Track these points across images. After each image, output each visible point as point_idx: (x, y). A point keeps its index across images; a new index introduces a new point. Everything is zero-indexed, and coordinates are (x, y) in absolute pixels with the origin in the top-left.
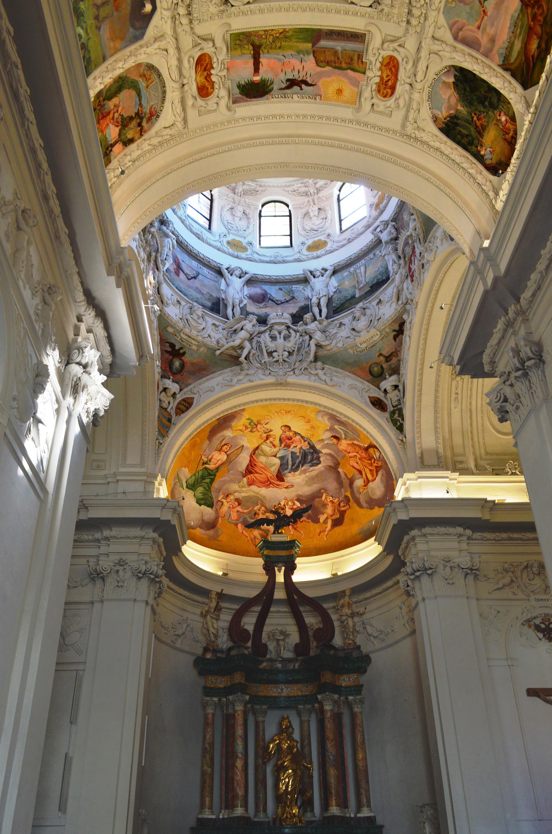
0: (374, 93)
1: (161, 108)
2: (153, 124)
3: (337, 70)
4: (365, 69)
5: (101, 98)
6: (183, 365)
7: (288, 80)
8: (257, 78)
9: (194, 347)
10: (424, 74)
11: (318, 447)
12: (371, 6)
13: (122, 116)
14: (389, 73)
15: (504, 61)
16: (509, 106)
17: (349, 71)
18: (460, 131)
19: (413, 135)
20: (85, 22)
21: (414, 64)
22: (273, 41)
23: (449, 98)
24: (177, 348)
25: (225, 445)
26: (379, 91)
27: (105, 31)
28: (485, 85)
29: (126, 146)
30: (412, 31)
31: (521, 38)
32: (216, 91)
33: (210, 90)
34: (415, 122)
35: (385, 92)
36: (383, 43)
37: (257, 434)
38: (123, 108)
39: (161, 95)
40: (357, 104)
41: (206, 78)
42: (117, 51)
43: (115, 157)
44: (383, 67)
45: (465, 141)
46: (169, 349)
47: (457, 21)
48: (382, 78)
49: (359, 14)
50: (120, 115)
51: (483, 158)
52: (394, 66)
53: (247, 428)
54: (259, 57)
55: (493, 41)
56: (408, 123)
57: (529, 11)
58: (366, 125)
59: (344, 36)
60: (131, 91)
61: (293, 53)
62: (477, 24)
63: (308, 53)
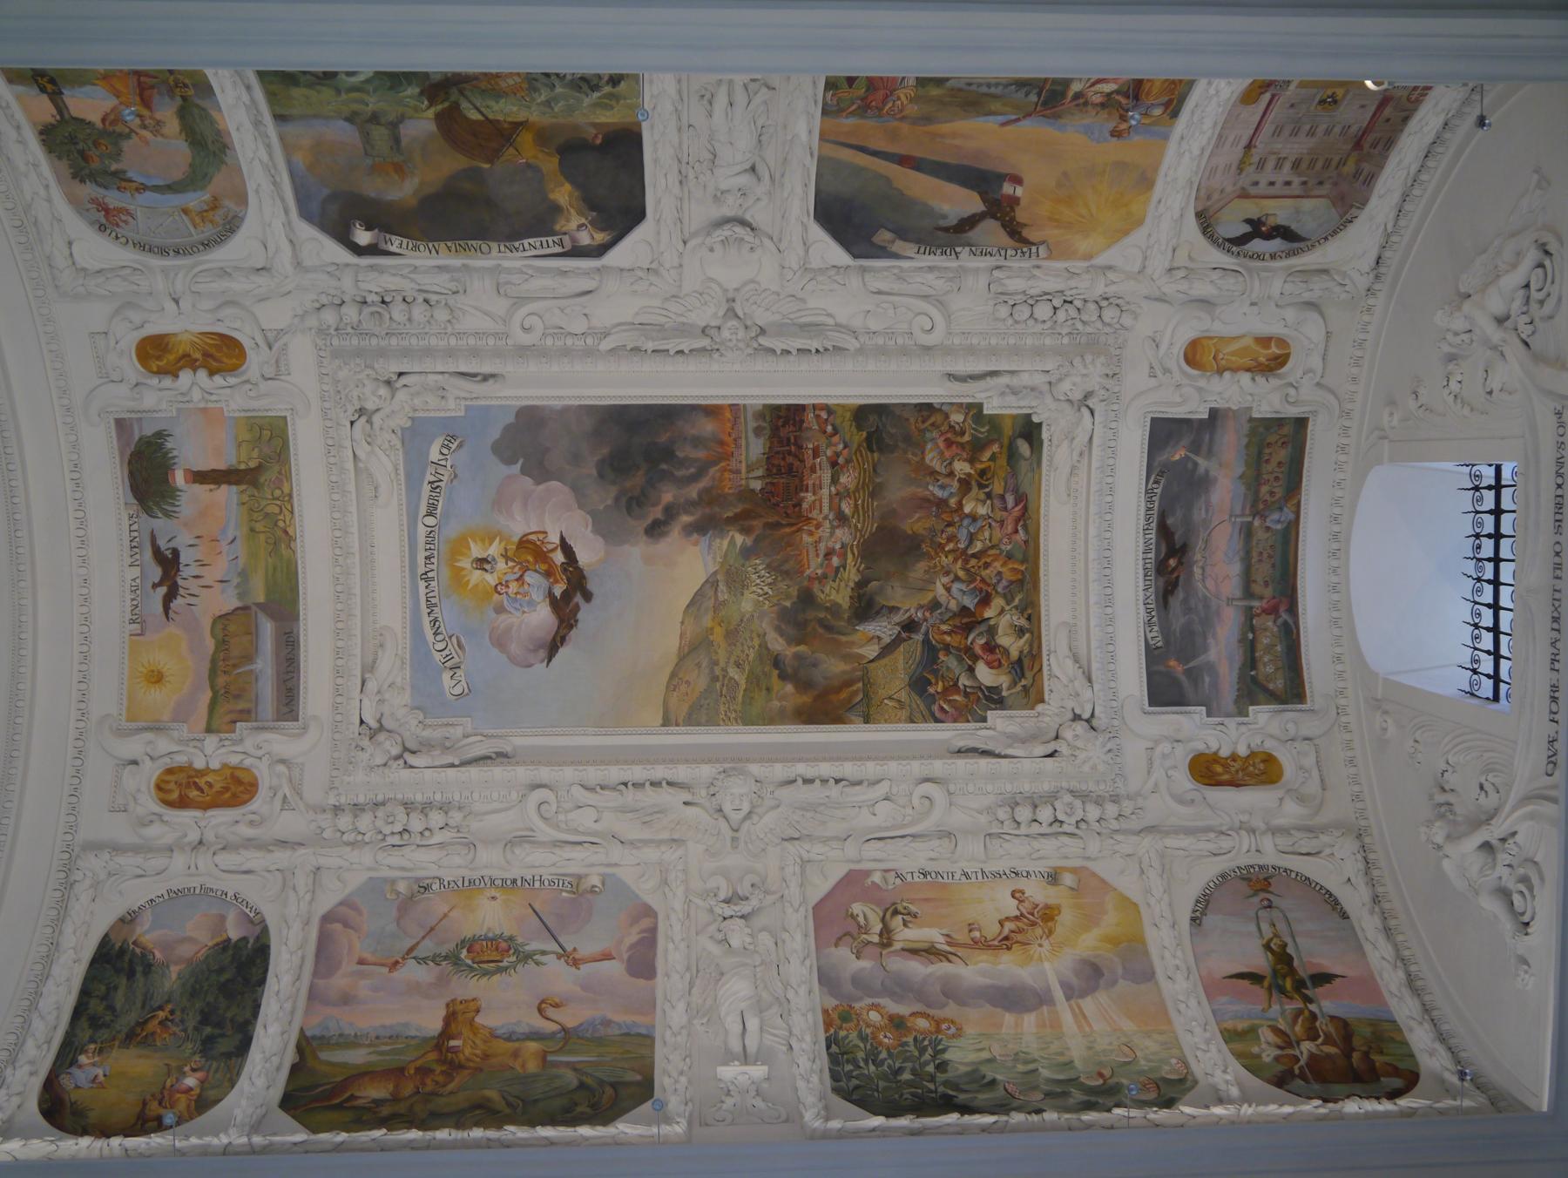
0: (167, 760)
1: (123, 240)
3: (206, 665)
4: (218, 731)
5: (191, 92)
7: (176, 552)
8: (179, 478)
10: (233, 868)
12: (362, 722)
13: (128, 137)
14: (218, 787)
15: (314, 1038)
16: (227, 1084)
17: (209, 694)
18: (116, 988)
19: (78, 876)
20: (375, 91)
21: (249, 840)
22: (267, 515)
23: (191, 940)
26: (170, 771)
27: (341, 133)
28: (248, 1015)
29: (41, 133)
30: (325, 820)
31: (374, 1058)
32: (154, 381)
33: (154, 365)
34: (110, 875)
35: (172, 786)
36: (283, 761)
38: (147, 143)
39: (158, 241)
40: (133, 725)
41: (186, 355)
42: (288, 148)
43: (18, 97)
44: (228, 772)
45: (96, 1006)
47: (360, 913)
48: (206, 771)
49: (339, 700)
50: (132, 131)
51: (71, 1065)
52: (234, 796)
54: (230, 483)
55: (346, 999)
56: (107, 856)
57: (433, 1056)
58: (80, 754)
59: (288, 672)
61: (241, 562)
62: (367, 956)
63: (241, 596)
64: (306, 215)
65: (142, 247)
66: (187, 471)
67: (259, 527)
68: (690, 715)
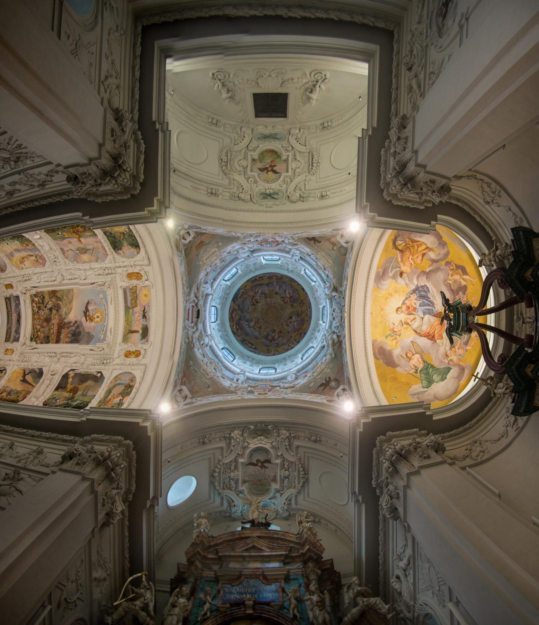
8: (141, 331)
11: (413, 287)
37: (403, 332)
53: (396, 338)
63: (133, 311)
68: (69, 292)
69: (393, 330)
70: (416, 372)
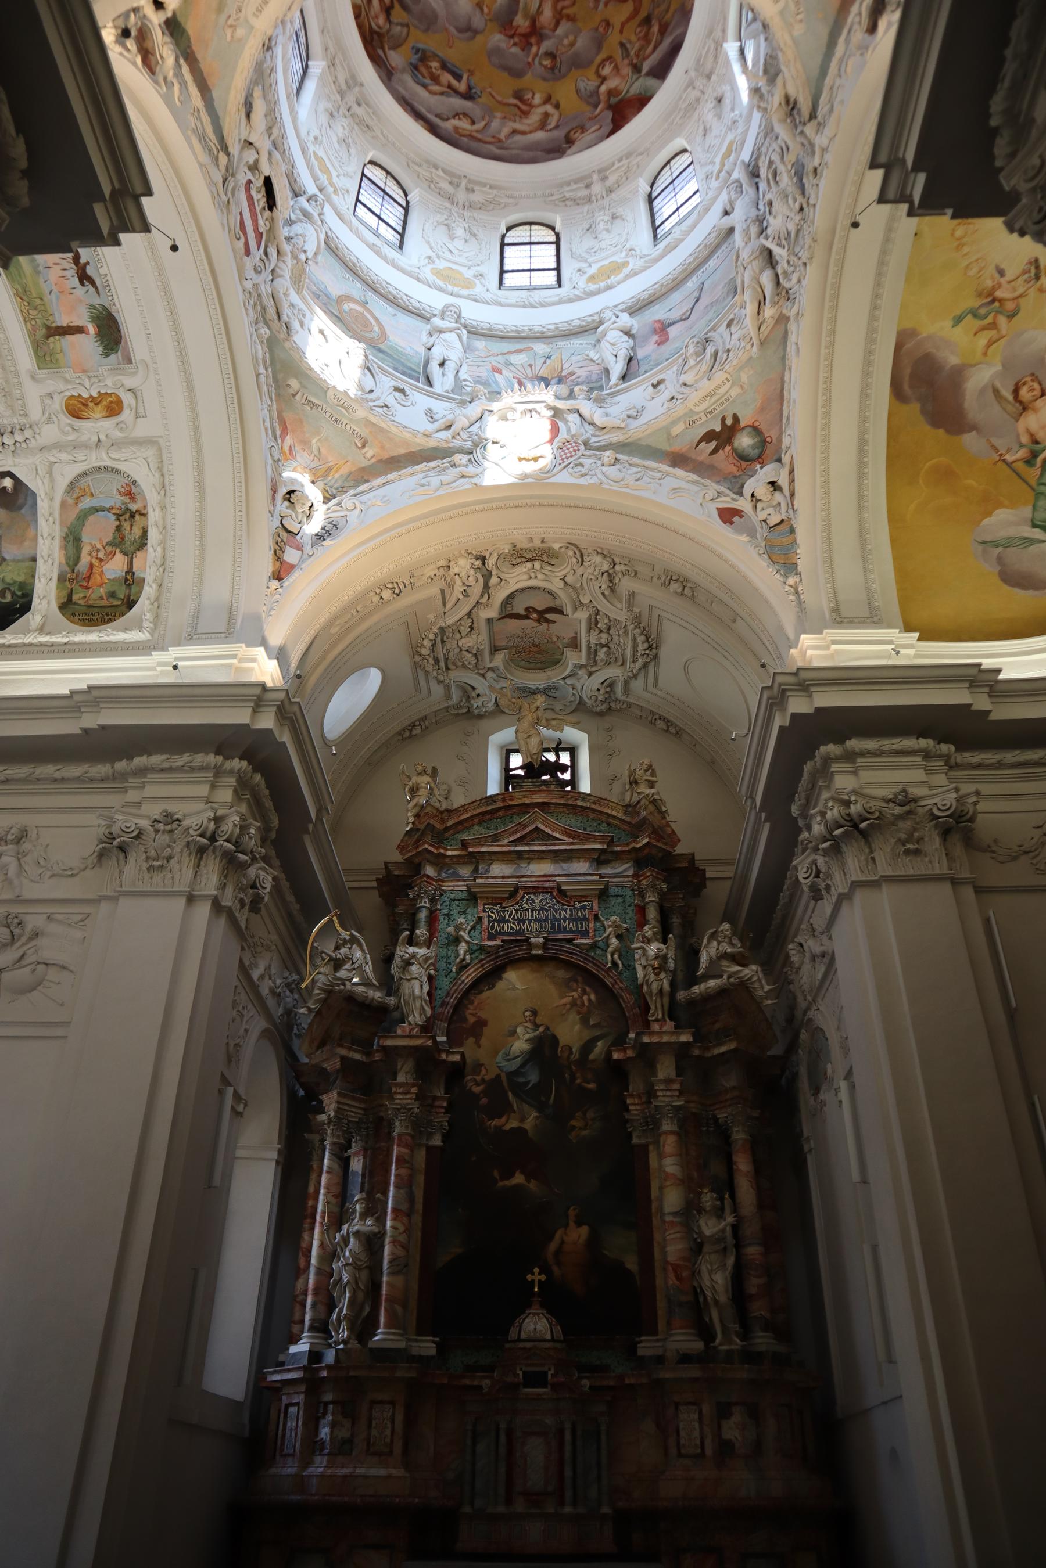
2: (141, 493)
6: (756, 430)
7: (83, 284)
8: (91, 328)
9: (734, 392)
13: (107, 544)
22: (36, 309)
24: (718, 429)
25: (1016, 391)
33: (113, 399)
39: (108, 475)
41: (96, 404)
46: (713, 444)
53: (993, 326)
54: (62, 327)
60: (88, 523)
64: (34, 494)
65: (116, 471)
66: (88, 333)
67: (38, 301)
69: (991, 293)
70: (1030, 461)
